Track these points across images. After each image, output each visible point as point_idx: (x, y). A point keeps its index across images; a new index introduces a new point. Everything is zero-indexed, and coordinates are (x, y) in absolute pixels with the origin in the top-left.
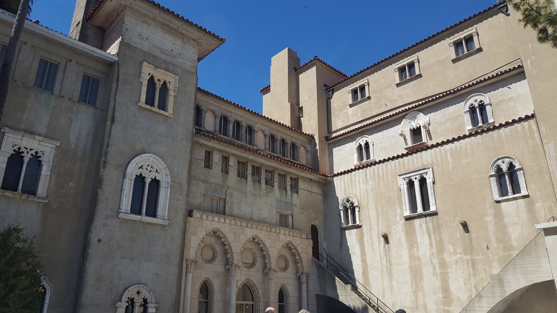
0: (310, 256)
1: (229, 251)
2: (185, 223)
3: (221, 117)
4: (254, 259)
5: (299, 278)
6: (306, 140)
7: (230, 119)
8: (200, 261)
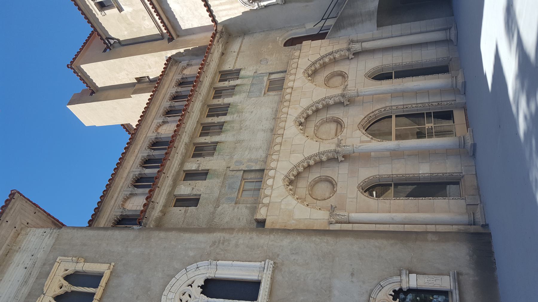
0: (325, 42)
1: (317, 158)
2: (273, 230)
3: (136, 186)
4: (331, 121)
5: (357, 54)
6: (175, 68)
7: (137, 173)
8: (332, 201)
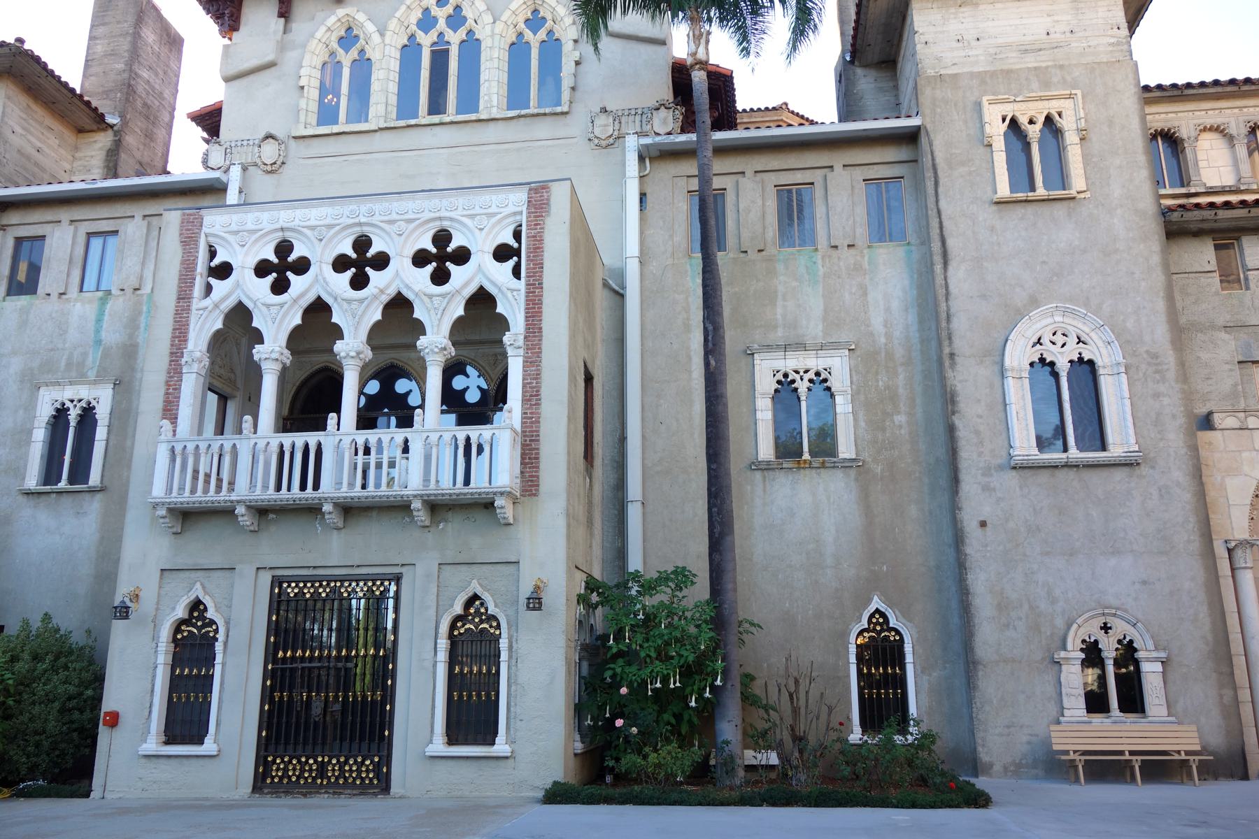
2: (1194, 449)
